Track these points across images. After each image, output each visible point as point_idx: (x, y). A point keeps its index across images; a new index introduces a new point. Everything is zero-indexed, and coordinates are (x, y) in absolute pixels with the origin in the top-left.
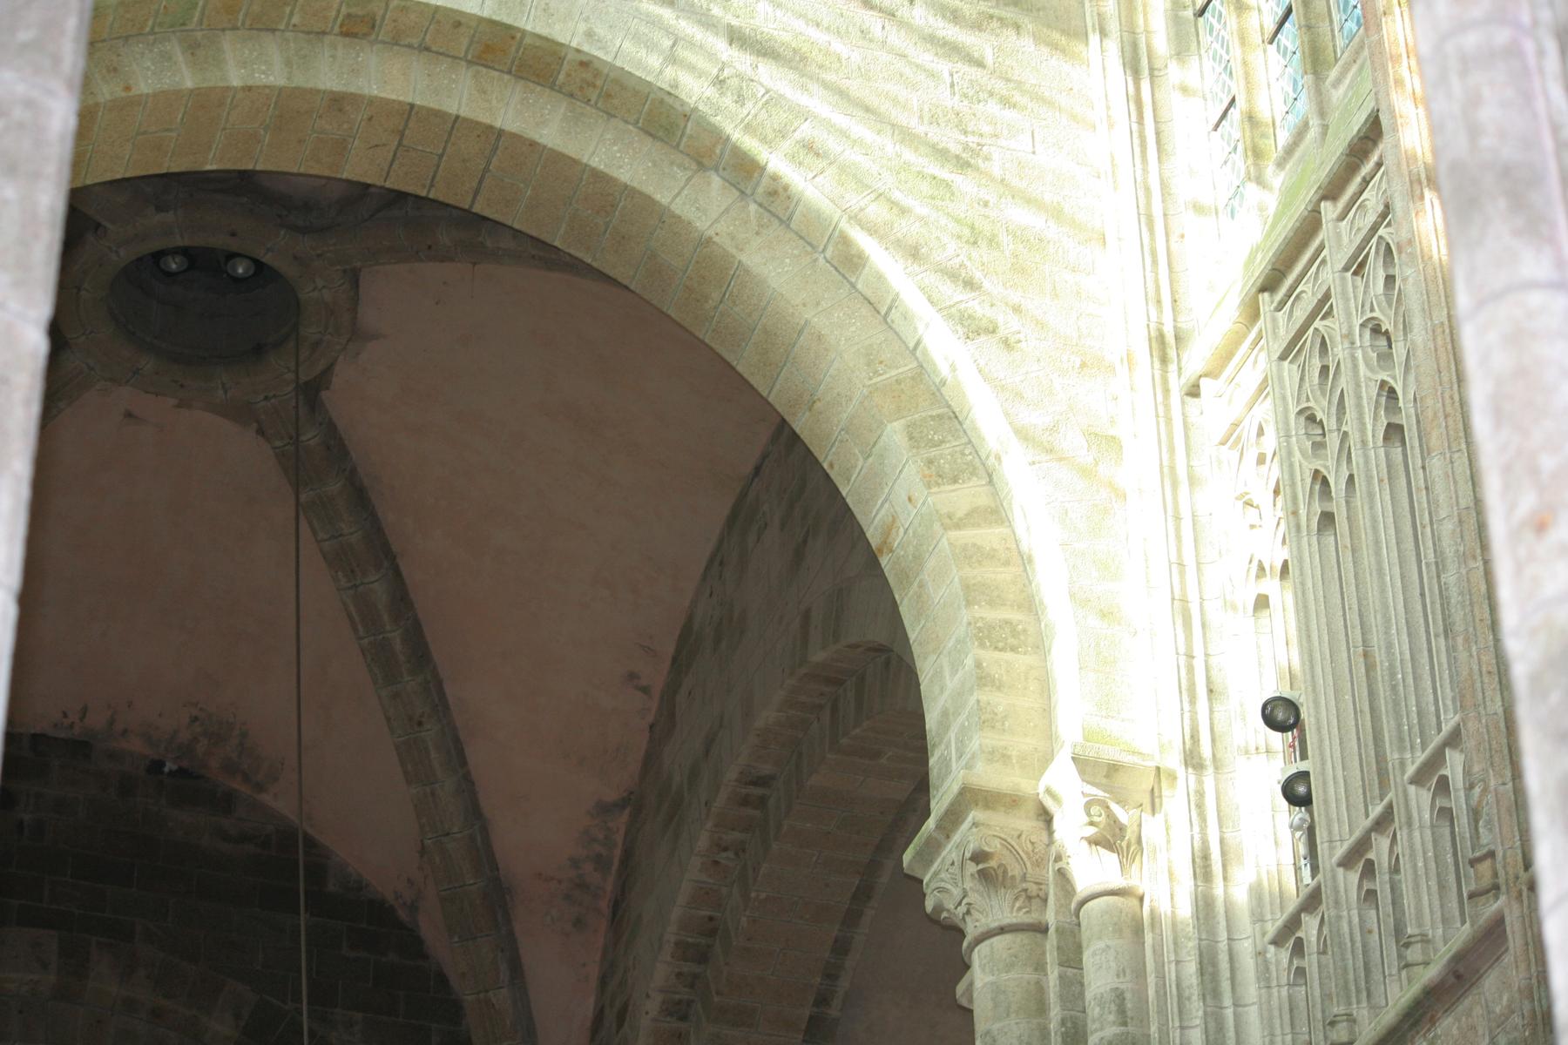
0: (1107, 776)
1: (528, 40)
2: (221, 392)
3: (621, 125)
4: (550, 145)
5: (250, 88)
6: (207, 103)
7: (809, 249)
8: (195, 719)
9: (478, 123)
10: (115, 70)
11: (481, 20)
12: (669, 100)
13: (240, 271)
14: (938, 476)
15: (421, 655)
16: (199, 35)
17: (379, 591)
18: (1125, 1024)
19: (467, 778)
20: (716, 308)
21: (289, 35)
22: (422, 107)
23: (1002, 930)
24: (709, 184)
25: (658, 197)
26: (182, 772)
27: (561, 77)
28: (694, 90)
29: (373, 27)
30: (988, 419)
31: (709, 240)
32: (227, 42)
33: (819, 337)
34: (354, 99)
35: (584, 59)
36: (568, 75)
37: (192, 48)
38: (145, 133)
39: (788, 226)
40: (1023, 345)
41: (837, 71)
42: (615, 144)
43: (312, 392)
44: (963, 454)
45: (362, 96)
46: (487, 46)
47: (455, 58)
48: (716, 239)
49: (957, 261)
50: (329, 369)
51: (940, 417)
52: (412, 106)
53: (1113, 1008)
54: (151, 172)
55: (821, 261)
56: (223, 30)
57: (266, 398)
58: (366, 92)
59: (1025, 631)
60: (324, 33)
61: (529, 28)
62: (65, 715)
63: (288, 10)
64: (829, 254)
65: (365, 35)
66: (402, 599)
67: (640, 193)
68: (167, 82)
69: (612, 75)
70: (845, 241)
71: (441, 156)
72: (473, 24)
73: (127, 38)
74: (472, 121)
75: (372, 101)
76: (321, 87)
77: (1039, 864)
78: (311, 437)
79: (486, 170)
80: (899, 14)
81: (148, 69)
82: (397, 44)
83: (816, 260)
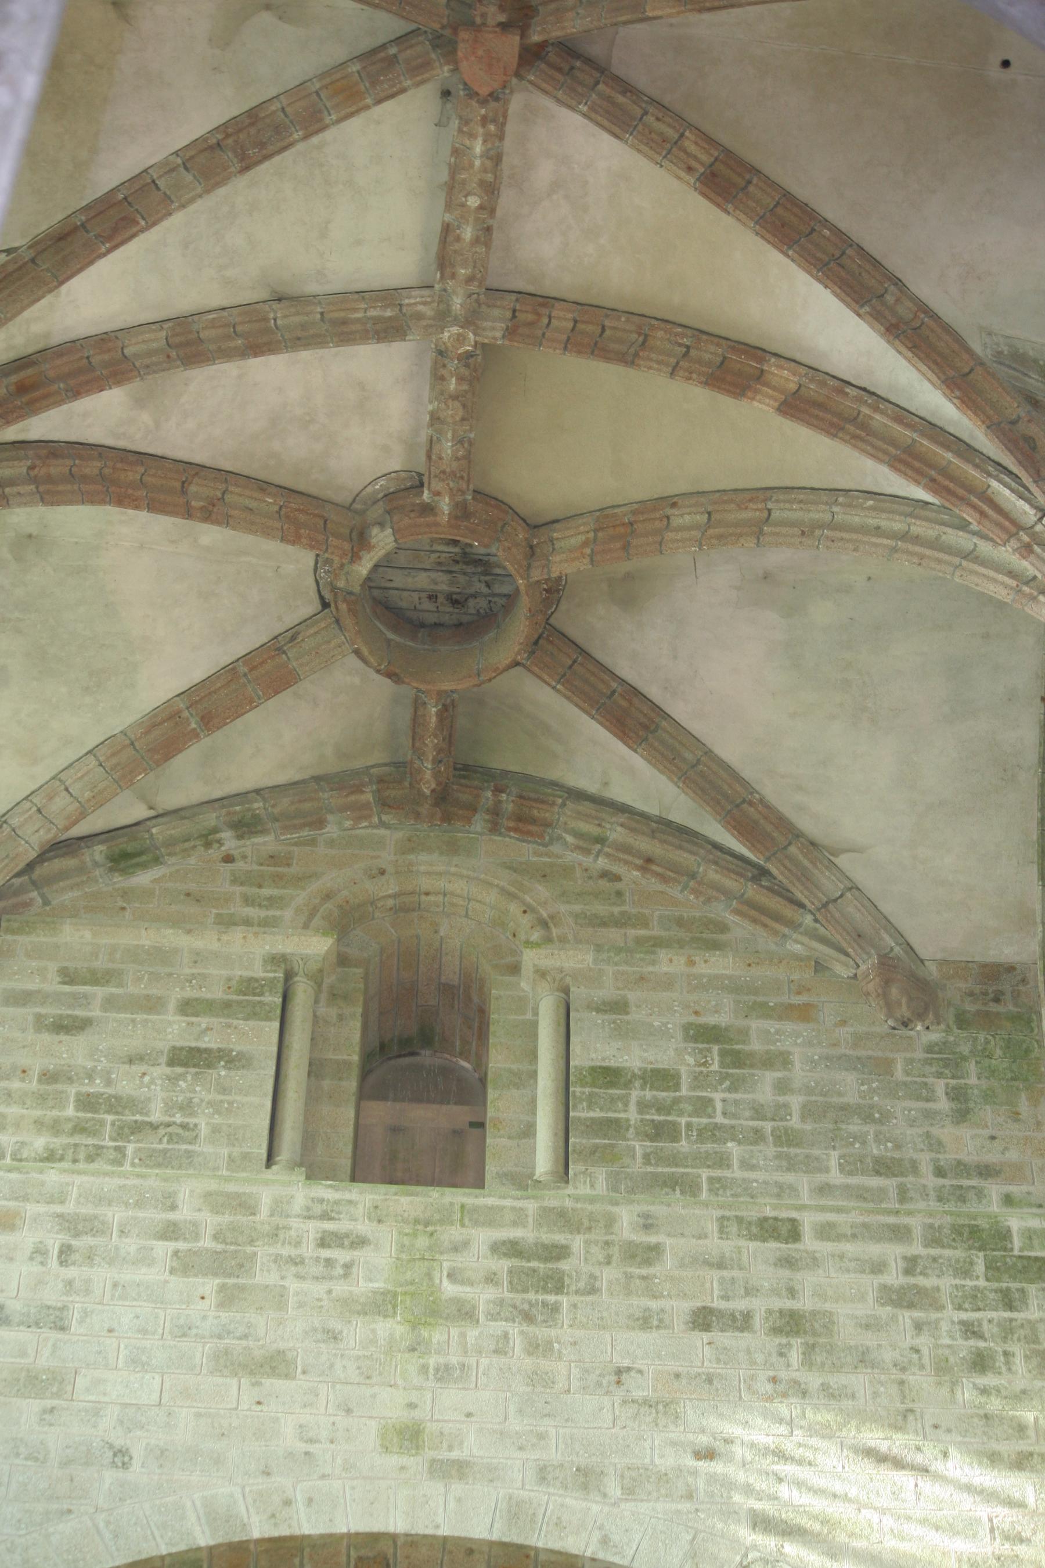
11: (491, 1544)
41: (868, 1538)
72: (486, 1549)
80: (932, 1468)
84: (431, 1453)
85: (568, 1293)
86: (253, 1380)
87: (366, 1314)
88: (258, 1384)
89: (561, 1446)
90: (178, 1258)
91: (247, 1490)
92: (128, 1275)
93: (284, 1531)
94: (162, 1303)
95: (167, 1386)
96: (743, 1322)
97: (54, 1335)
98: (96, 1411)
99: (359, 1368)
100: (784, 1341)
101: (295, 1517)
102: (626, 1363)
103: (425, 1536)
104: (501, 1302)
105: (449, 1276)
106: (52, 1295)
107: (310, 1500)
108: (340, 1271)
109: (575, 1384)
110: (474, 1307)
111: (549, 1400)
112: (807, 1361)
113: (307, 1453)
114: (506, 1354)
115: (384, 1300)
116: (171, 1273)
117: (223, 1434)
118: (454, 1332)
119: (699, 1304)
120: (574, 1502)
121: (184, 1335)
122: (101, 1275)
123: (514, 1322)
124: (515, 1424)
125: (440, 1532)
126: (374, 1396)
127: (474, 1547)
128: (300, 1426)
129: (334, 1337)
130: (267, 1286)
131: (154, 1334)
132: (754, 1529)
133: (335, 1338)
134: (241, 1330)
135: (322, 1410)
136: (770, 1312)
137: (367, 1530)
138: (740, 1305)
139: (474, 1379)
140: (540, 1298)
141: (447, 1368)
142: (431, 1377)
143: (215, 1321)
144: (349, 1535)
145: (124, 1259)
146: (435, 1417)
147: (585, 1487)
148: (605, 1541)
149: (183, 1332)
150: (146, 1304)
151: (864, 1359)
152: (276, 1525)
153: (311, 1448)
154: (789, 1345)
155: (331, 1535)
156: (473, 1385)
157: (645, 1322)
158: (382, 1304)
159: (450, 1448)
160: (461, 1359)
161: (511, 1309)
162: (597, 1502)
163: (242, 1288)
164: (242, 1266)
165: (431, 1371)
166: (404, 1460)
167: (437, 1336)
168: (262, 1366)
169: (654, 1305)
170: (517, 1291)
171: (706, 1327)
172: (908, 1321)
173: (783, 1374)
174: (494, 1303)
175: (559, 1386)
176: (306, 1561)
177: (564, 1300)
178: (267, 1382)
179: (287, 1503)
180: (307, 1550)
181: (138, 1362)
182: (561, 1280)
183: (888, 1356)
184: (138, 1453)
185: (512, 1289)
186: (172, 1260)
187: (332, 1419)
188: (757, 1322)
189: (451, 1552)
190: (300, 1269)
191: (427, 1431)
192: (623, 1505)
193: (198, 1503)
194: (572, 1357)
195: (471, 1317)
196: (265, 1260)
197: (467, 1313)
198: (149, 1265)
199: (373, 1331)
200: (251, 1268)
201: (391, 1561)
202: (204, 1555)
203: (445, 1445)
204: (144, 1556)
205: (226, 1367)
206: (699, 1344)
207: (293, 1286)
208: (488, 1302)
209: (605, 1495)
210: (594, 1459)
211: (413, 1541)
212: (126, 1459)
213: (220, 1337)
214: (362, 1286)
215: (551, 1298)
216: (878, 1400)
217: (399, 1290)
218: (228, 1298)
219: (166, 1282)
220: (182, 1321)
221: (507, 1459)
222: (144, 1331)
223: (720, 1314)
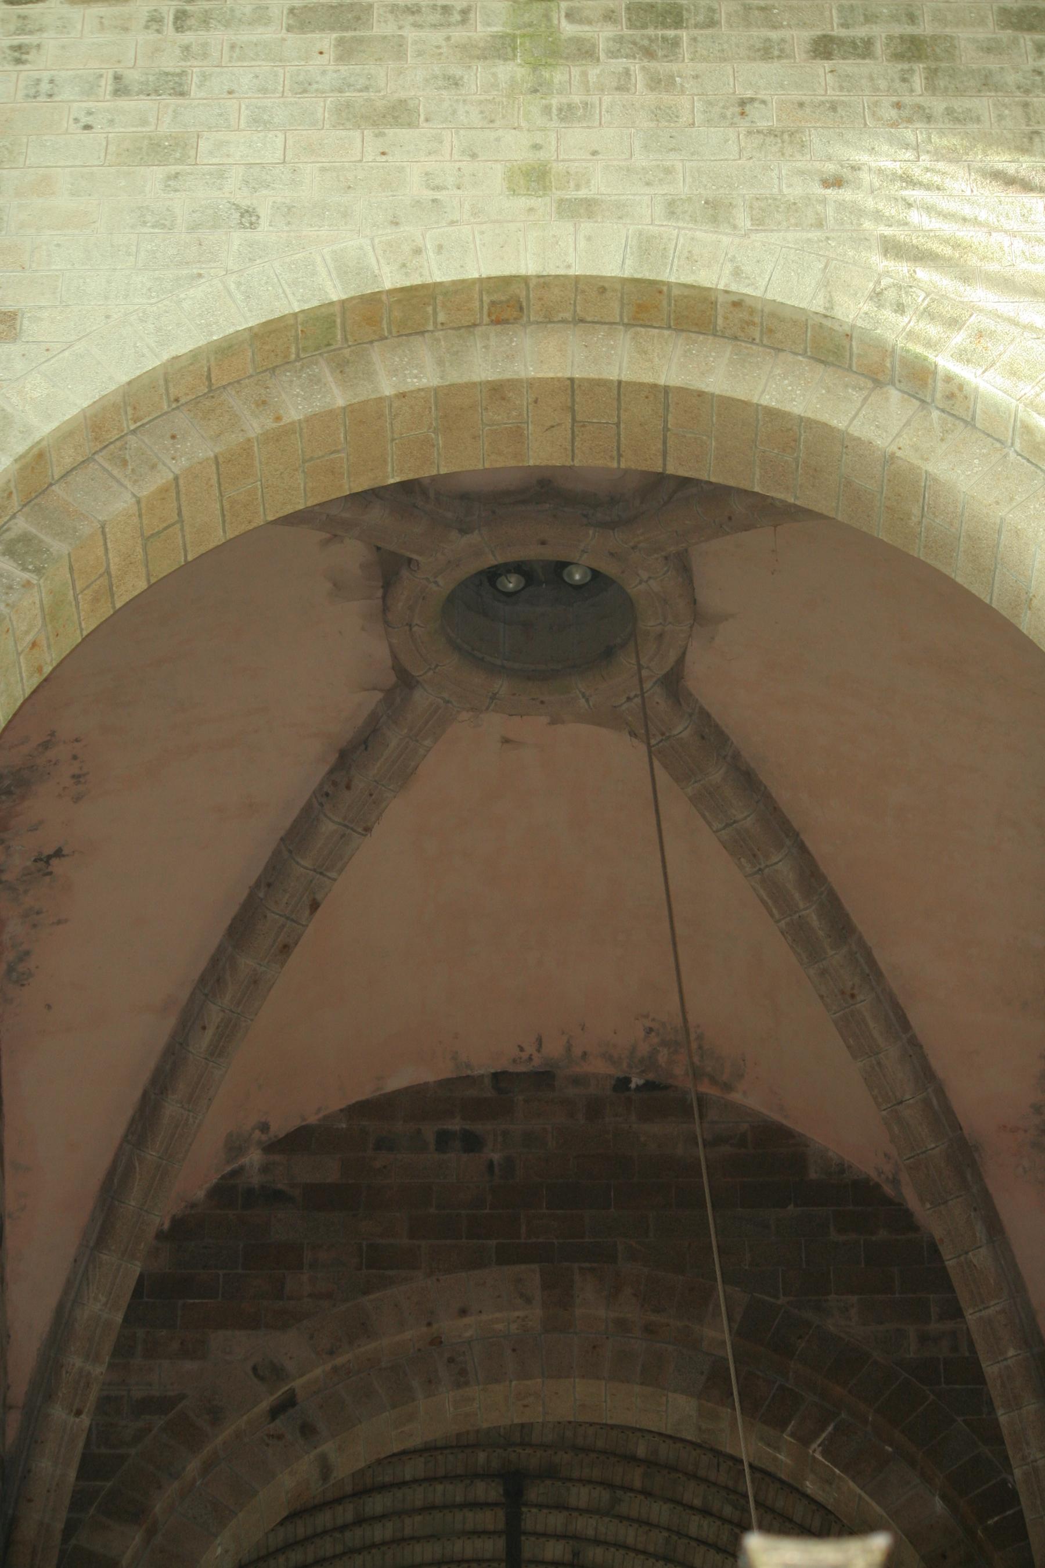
1: (675, 292)
2: (583, 701)
3: (790, 358)
4: (717, 392)
5: (404, 395)
6: (364, 418)
7: (998, 445)
8: (651, 1030)
9: (641, 384)
10: (264, 403)
11: (624, 281)
12: (828, 323)
13: (577, 577)
15: (842, 926)
16: (346, 352)
17: (784, 869)
19: (914, 1043)
20: (920, 523)
21: (439, 334)
22: (582, 379)
24: (887, 399)
25: (834, 423)
27: (720, 321)
28: (852, 311)
29: (521, 309)
31: (893, 456)
32: (376, 354)
33: (1017, 533)
34: (514, 384)
35: (735, 299)
36: (726, 318)
37: (341, 367)
38: (312, 459)
39: (974, 427)
41: (999, 260)
43: (673, 682)
45: (519, 381)
46: (639, 306)
48: (899, 454)
50: (681, 660)
52: (572, 380)
54: (333, 497)
55: (1012, 455)
56: (371, 342)
57: (629, 699)
58: (523, 375)
60: (475, 325)
61: (673, 279)
63: (430, 309)
64: (1018, 446)
66: (811, 875)
67: (817, 422)
68: (318, 405)
69: (766, 310)
71: (618, 425)
72: (618, 287)
73: (274, 369)
74: (635, 384)
75: (531, 383)
76: (476, 379)
78: (683, 730)
79: (666, 429)
81: (297, 395)
82: (550, 322)
83: (1006, 456)
84: (559, 193)
85: (687, 28)
86: (377, 131)
87: (486, 58)
88: (382, 134)
89: (689, 180)
90: (294, 15)
91: (377, 241)
92: (245, 36)
93: (416, 280)
94: (281, 61)
95: (290, 142)
96: (864, 49)
97: (174, 101)
98: (221, 174)
99: (482, 112)
100: (906, 66)
101: (426, 264)
102: (749, 94)
104: (620, 40)
105: (567, 16)
106: (170, 62)
107: (440, 247)
108: (457, 17)
109: (699, 118)
110: (594, 46)
111: (674, 134)
112: (931, 87)
113: (434, 201)
114: (628, 90)
115: (503, 44)
116: (288, 30)
117: (349, 187)
118: (576, 71)
119: (819, 33)
120: (704, 235)
121: (305, 91)
122: (218, 37)
123: (635, 58)
124: (641, 160)
125: (571, 272)
126: (498, 139)
127: (606, 285)
128: (426, 174)
129: (456, 83)
130: (386, 37)
131: (274, 91)
132: (885, 255)
133: (456, 84)
134: (362, 82)
135: (448, 157)
136: (890, 38)
137: (499, 274)
138: (861, 32)
139: (597, 117)
140: (660, 33)
141: (570, 107)
142: (555, 117)
143: (335, 75)
144: (480, 280)
145: (240, 20)
146: (561, 157)
147: (714, 220)
148: (737, 273)
149: (303, 88)
150: (264, 63)
151: (987, 82)
152: (407, 274)
153: (438, 195)
154: (911, 71)
155: (463, 281)
156: (597, 123)
157: (766, 52)
158: (501, 48)
159: (578, 187)
160: (584, 98)
161: (631, 46)
162: (726, 234)
163: (360, 41)
164: (358, 18)
165: (554, 111)
166: (532, 202)
167: (558, 76)
168: (384, 117)
169: (774, 35)
170: (636, 28)
171: (828, 56)
172: (1029, 43)
173: (907, 100)
174: (614, 40)
175: (683, 120)
176: (439, 308)
177: (684, 35)
178: (391, 132)
179: (418, 251)
180: (440, 298)
181: (260, 122)
182: (679, 15)
183: (1011, 78)
184: (264, 212)
185: (631, 25)
186: (288, 18)
187: (458, 165)
188: (878, 48)
189: (583, 292)
190: (417, 18)
191: (553, 171)
192: (753, 236)
193: (327, 257)
194: (695, 91)
195: (591, 56)
196: (381, 11)
197: (587, 52)
198: (266, 24)
199: (494, 75)
200: (368, 20)
201: (524, 304)
202: (337, 309)
203: (572, 184)
205: (348, 120)
206: (821, 72)
207: (411, 35)
208: (608, 39)
209: (735, 227)
210: (722, 191)
211: (545, 282)
212: (254, 219)
213: (341, 91)
214: (481, 31)
215: (671, 33)
216: (1003, 123)
217: (518, 32)
218: (346, 52)
219: (284, 40)
220: (301, 78)
221: (634, 195)
222: (264, 90)
223: (841, 42)
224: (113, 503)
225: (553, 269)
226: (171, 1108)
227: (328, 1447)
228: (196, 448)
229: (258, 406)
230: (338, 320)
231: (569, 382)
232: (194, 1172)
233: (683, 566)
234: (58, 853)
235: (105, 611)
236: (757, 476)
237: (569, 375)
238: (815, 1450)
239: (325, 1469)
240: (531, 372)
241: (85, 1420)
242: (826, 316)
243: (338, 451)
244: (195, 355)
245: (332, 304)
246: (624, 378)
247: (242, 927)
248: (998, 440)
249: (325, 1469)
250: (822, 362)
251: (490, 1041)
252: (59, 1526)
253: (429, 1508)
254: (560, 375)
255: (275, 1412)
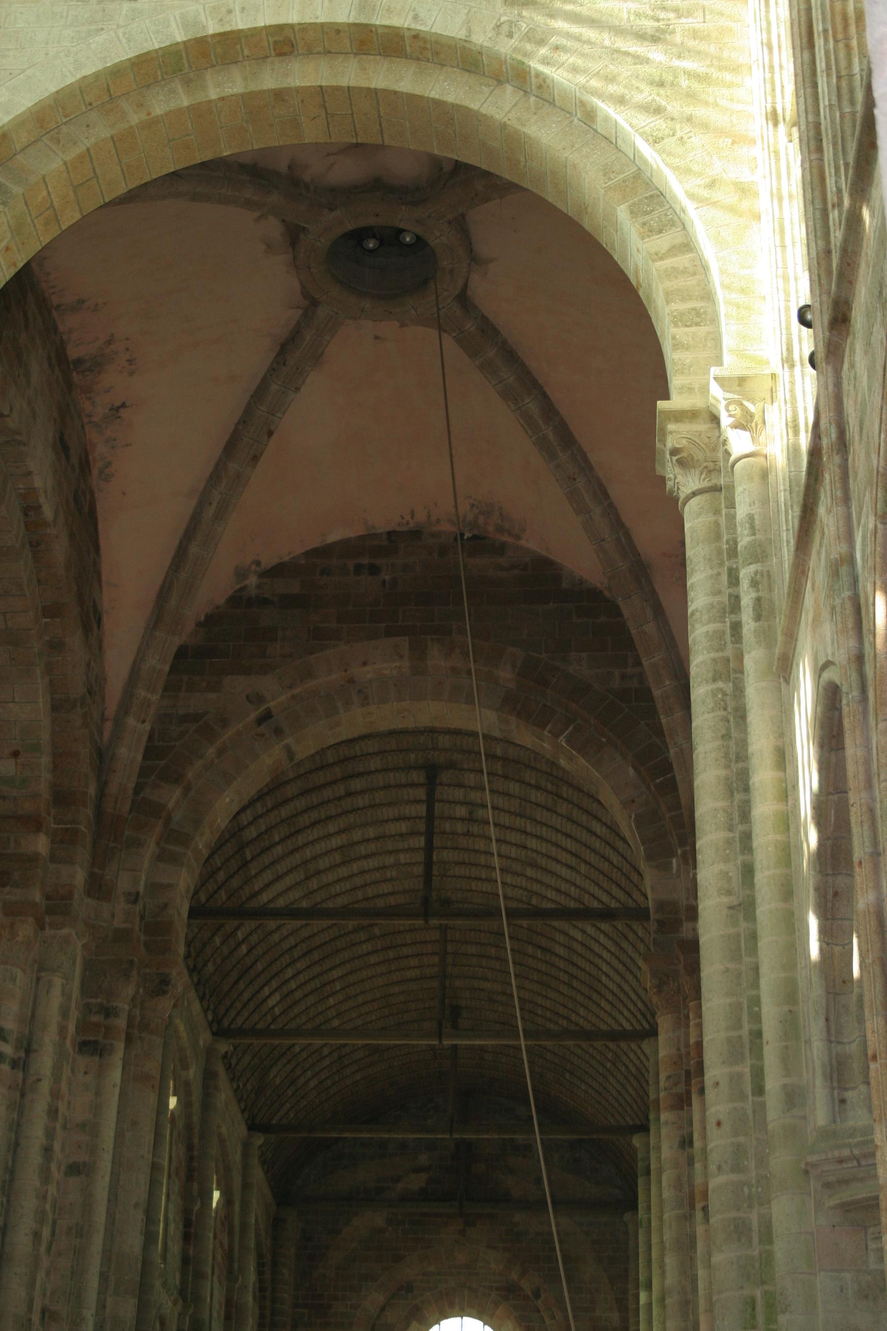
0: (740, 385)
2: (413, 311)
3: (450, 69)
4: (405, 91)
7: (568, 115)
8: (473, 505)
9: (361, 88)
10: (142, 105)
12: (467, 45)
13: (408, 239)
14: (649, 231)
15: (567, 438)
16: (192, 75)
17: (533, 406)
18: (754, 534)
19: (611, 505)
20: (525, 166)
21: (246, 63)
23: (694, 494)
25: (472, 106)
26: (475, 537)
27: (408, 48)
28: (481, 39)
29: (293, 45)
30: (677, 188)
32: (209, 75)
34: (288, 90)
35: (414, 34)
36: (411, 46)
37: (187, 82)
38: (174, 139)
39: (555, 105)
40: (693, 139)
42: (445, 81)
43: (463, 299)
44: (666, 215)
45: (290, 88)
47: (346, 53)
48: (509, 123)
49: (650, 98)
50: (466, 286)
51: (651, 196)
52: (321, 87)
53: (748, 525)
54: (191, 164)
55: (576, 121)
56: (206, 69)
58: (292, 85)
59: (705, 312)
60: (267, 57)
61: (378, 23)
62: (402, 518)
63: (238, 47)
64: (579, 115)
65: (291, 52)
66: (549, 409)
67: (462, 106)
68: (173, 105)
69: (433, 39)
70: (583, 104)
71: (352, 115)
72: (347, 29)
73: (149, 86)
75: (298, 90)
76: (265, 88)
77: (714, 449)
78: (470, 326)
79: (380, 117)
82: (311, 54)
91: (207, 6)
93: (227, 28)
103: (310, 24)
125: (318, 21)
137: (276, 23)
144: (265, 27)
148: (416, 17)
152: (222, 25)
155: (255, 28)
179: (230, 12)
180: (243, 40)
189: (327, 33)
193: (177, 17)
202: (182, 47)
204: (145, 51)
211: (304, 28)
224: (50, 163)
225: (308, 20)
226: (194, 549)
227: (289, 740)
228: (102, 131)
229: (138, 107)
230: (184, 55)
231: (319, 89)
232: (213, 588)
233: (461, 226)
234: (123, 405)
235: (54, 232)
236: (435, 144)
237: (319, 84)
238: (562, 740)
239: (291, 755)
240: (298, 83)
241: (148, 726)
242: (466, 41)
243: (188, 135)
244: (97, 76)
245: (178, 43)
246: (351, 85)
247: (231, 447)
248: (568, 112)
249: (291, 755)
250: (468, 71)
251: (384, 514)
252: (132, 785)
253: (387, 787)
254: (314, 84)
255: (261, 721)
